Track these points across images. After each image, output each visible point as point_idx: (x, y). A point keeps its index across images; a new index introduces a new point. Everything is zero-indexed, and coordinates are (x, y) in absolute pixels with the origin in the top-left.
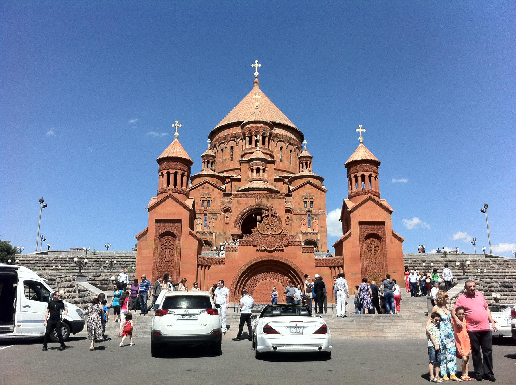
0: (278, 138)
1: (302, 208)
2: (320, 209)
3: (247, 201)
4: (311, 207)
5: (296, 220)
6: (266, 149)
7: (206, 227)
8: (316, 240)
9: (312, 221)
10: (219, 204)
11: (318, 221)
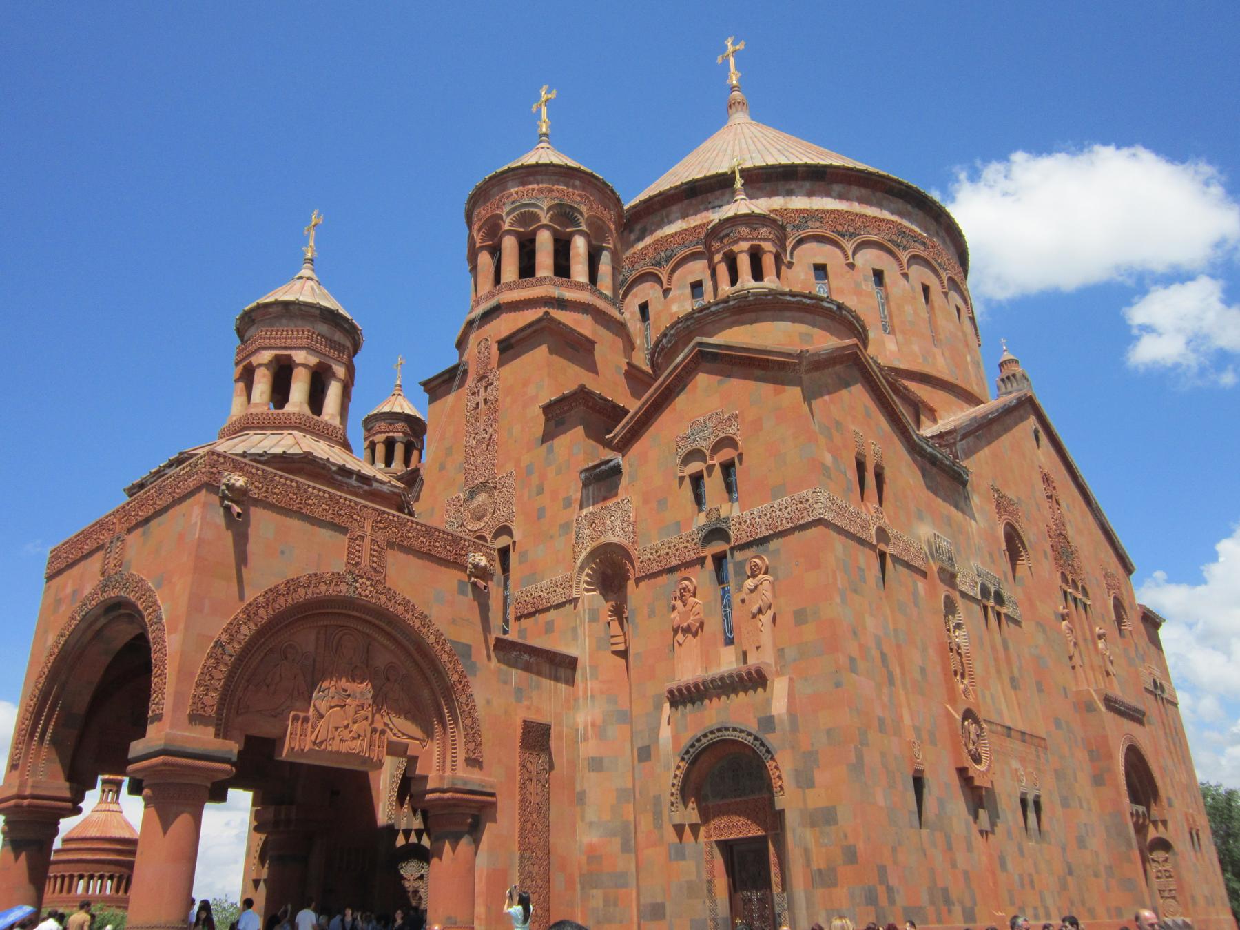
1: (678, 526)
2: (776, 493)
5: (652, 614)
6: (577, 286)
8: (753, 728)
9: (740, 588)
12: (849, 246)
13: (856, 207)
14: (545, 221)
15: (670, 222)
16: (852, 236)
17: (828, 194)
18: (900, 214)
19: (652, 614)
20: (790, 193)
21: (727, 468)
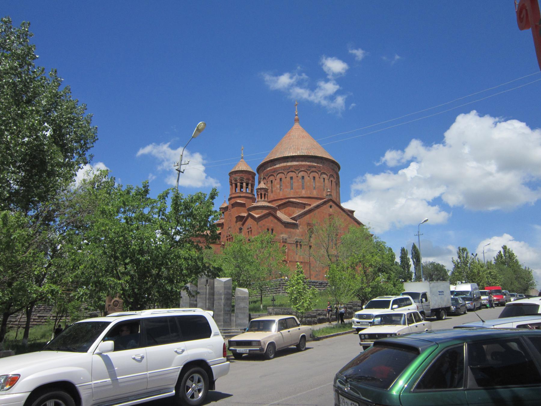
0: (277, 172)
12: (297, 173)
13: (301, 163)
14: (238, 181)
15: (269, 168)
16: (298, 170)
17: (295, 161)
18: (310, 162)
20: (288, 162)
21: (251, 231)
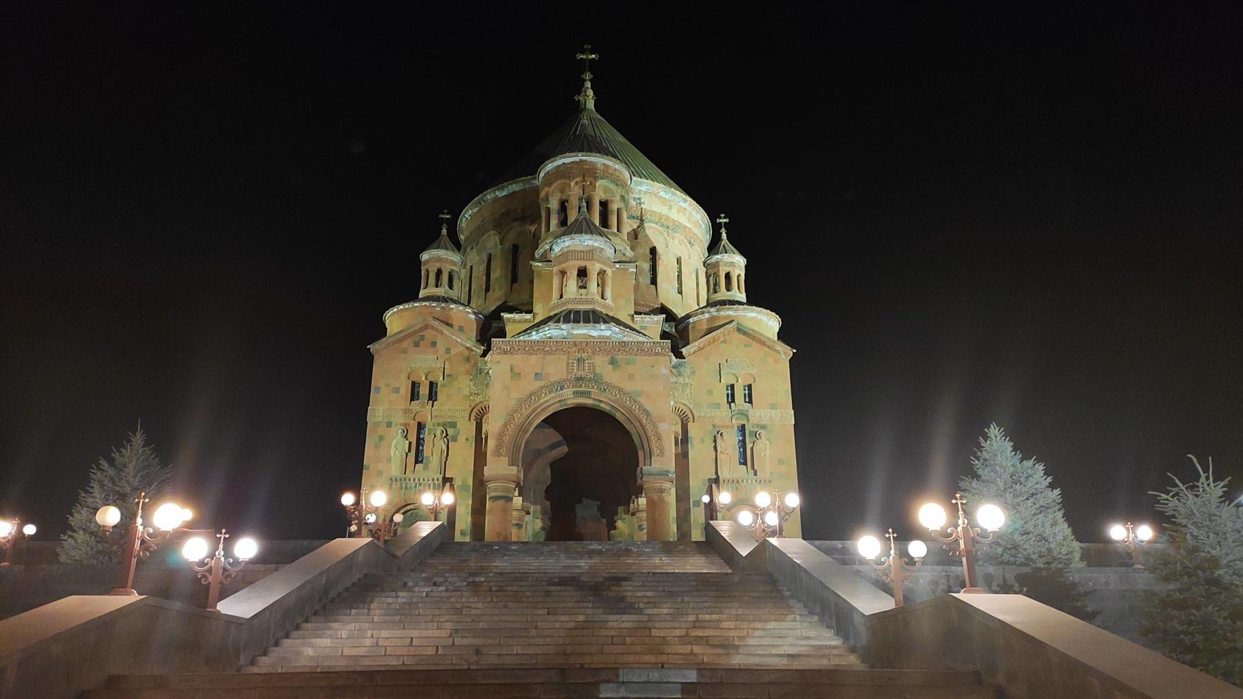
2: (773, 406)
3: (542, 368)
4: (745, 402)
7: (421, 462)
10: (465, 394)
11: (770, 444)
19: (702, 441)
